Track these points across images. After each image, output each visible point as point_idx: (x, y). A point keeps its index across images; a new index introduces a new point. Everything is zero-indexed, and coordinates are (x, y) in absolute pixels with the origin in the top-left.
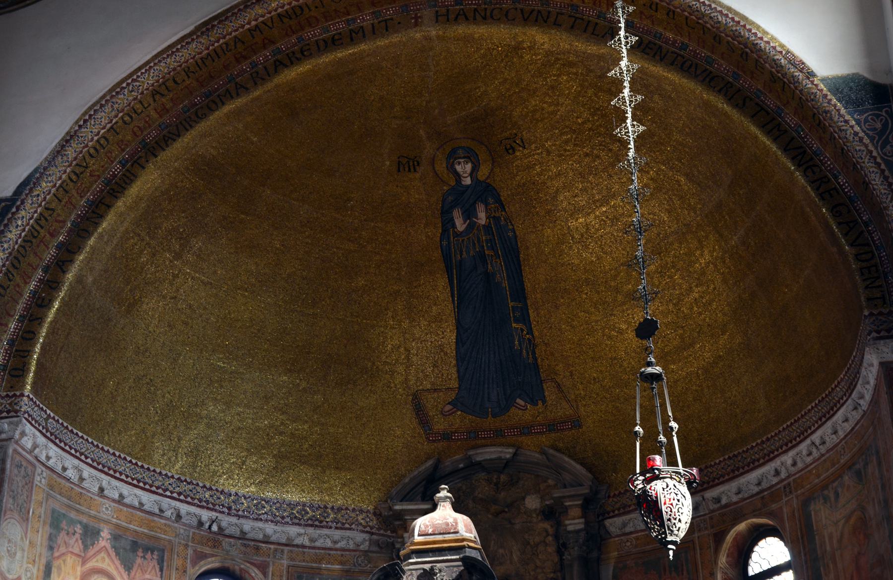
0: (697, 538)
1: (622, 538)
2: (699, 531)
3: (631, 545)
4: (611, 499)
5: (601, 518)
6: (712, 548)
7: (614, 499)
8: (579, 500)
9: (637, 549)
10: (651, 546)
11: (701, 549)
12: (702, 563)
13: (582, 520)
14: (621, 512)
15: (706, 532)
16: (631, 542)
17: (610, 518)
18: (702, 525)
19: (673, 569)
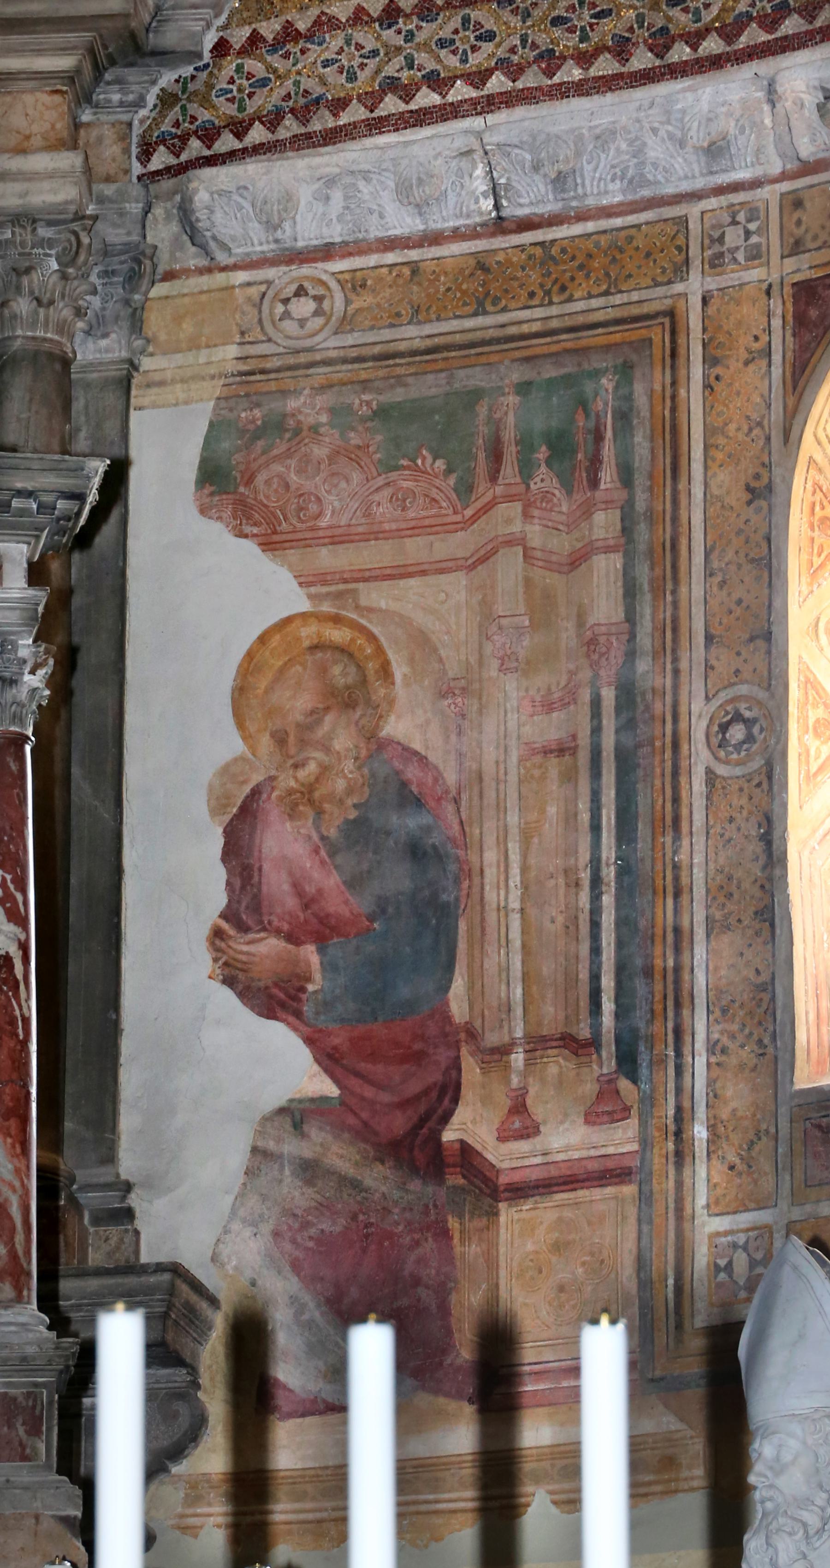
0: (695, 301)
1: (271, 273)
2: (716, 263)
3: (317, 313)
4: (229, 66)
5: (161, 159)
6: (777, 358)
7: (253, 65)
8: (63, 50)
9: (350, 339)
10: (428, 329)
11: (710, 361)
12: (709, 431)
13: (69, 160)
14: (283, 133)
15: (755, 274)
16: (319, 299)
17: (211, 161)
18: (733, 237)
19: (542, 453)
